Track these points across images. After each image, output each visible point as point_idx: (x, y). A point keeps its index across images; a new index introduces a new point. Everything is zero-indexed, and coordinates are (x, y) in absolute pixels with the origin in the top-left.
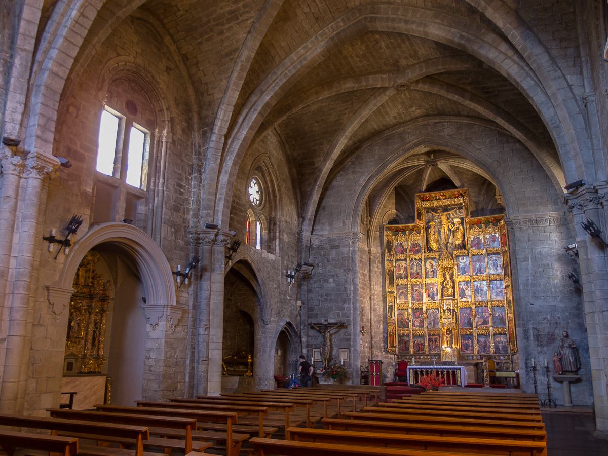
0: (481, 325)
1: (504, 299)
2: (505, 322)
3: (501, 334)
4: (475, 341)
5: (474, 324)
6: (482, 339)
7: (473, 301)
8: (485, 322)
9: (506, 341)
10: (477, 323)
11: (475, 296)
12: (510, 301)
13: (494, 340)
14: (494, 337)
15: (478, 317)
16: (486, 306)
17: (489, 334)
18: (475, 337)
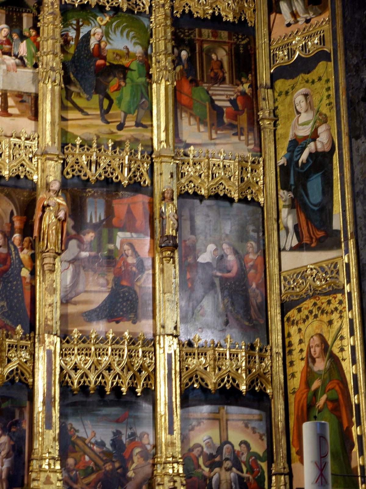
0: (90, 316)
1: (259, 150)
2: (264, 308)
3: (228, 395)
4: (46, 443)
5: (48, 308)
6: (96, 432)
7: (48, 137)
8: (123, 304)
9: (258, 447)
10: (66, 302)
11: (63, 108)
12: (321, 162)
13: (184, 439)
14: (184, 420)
15: (74, 261)
16: (135, 187)
17: (150, 394)
18: (48, 401)
